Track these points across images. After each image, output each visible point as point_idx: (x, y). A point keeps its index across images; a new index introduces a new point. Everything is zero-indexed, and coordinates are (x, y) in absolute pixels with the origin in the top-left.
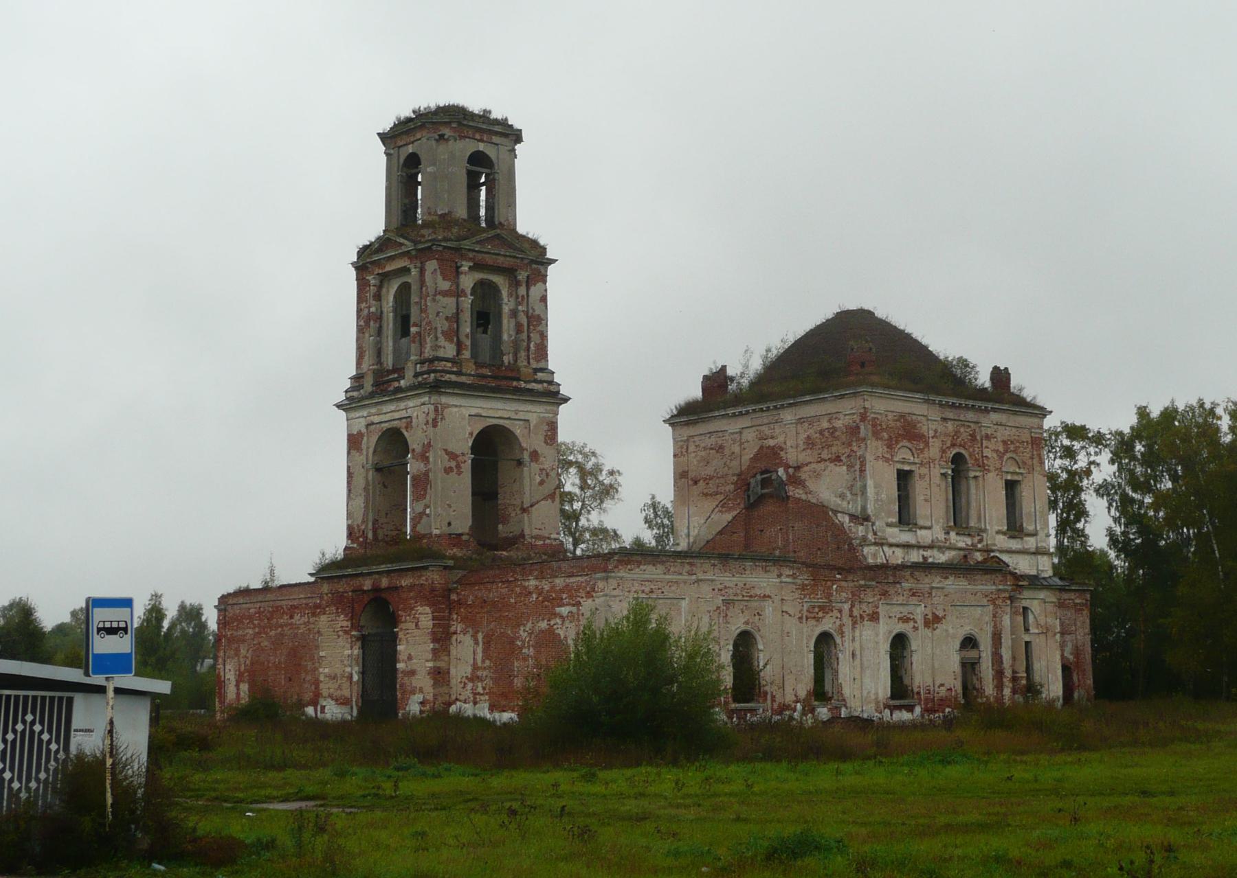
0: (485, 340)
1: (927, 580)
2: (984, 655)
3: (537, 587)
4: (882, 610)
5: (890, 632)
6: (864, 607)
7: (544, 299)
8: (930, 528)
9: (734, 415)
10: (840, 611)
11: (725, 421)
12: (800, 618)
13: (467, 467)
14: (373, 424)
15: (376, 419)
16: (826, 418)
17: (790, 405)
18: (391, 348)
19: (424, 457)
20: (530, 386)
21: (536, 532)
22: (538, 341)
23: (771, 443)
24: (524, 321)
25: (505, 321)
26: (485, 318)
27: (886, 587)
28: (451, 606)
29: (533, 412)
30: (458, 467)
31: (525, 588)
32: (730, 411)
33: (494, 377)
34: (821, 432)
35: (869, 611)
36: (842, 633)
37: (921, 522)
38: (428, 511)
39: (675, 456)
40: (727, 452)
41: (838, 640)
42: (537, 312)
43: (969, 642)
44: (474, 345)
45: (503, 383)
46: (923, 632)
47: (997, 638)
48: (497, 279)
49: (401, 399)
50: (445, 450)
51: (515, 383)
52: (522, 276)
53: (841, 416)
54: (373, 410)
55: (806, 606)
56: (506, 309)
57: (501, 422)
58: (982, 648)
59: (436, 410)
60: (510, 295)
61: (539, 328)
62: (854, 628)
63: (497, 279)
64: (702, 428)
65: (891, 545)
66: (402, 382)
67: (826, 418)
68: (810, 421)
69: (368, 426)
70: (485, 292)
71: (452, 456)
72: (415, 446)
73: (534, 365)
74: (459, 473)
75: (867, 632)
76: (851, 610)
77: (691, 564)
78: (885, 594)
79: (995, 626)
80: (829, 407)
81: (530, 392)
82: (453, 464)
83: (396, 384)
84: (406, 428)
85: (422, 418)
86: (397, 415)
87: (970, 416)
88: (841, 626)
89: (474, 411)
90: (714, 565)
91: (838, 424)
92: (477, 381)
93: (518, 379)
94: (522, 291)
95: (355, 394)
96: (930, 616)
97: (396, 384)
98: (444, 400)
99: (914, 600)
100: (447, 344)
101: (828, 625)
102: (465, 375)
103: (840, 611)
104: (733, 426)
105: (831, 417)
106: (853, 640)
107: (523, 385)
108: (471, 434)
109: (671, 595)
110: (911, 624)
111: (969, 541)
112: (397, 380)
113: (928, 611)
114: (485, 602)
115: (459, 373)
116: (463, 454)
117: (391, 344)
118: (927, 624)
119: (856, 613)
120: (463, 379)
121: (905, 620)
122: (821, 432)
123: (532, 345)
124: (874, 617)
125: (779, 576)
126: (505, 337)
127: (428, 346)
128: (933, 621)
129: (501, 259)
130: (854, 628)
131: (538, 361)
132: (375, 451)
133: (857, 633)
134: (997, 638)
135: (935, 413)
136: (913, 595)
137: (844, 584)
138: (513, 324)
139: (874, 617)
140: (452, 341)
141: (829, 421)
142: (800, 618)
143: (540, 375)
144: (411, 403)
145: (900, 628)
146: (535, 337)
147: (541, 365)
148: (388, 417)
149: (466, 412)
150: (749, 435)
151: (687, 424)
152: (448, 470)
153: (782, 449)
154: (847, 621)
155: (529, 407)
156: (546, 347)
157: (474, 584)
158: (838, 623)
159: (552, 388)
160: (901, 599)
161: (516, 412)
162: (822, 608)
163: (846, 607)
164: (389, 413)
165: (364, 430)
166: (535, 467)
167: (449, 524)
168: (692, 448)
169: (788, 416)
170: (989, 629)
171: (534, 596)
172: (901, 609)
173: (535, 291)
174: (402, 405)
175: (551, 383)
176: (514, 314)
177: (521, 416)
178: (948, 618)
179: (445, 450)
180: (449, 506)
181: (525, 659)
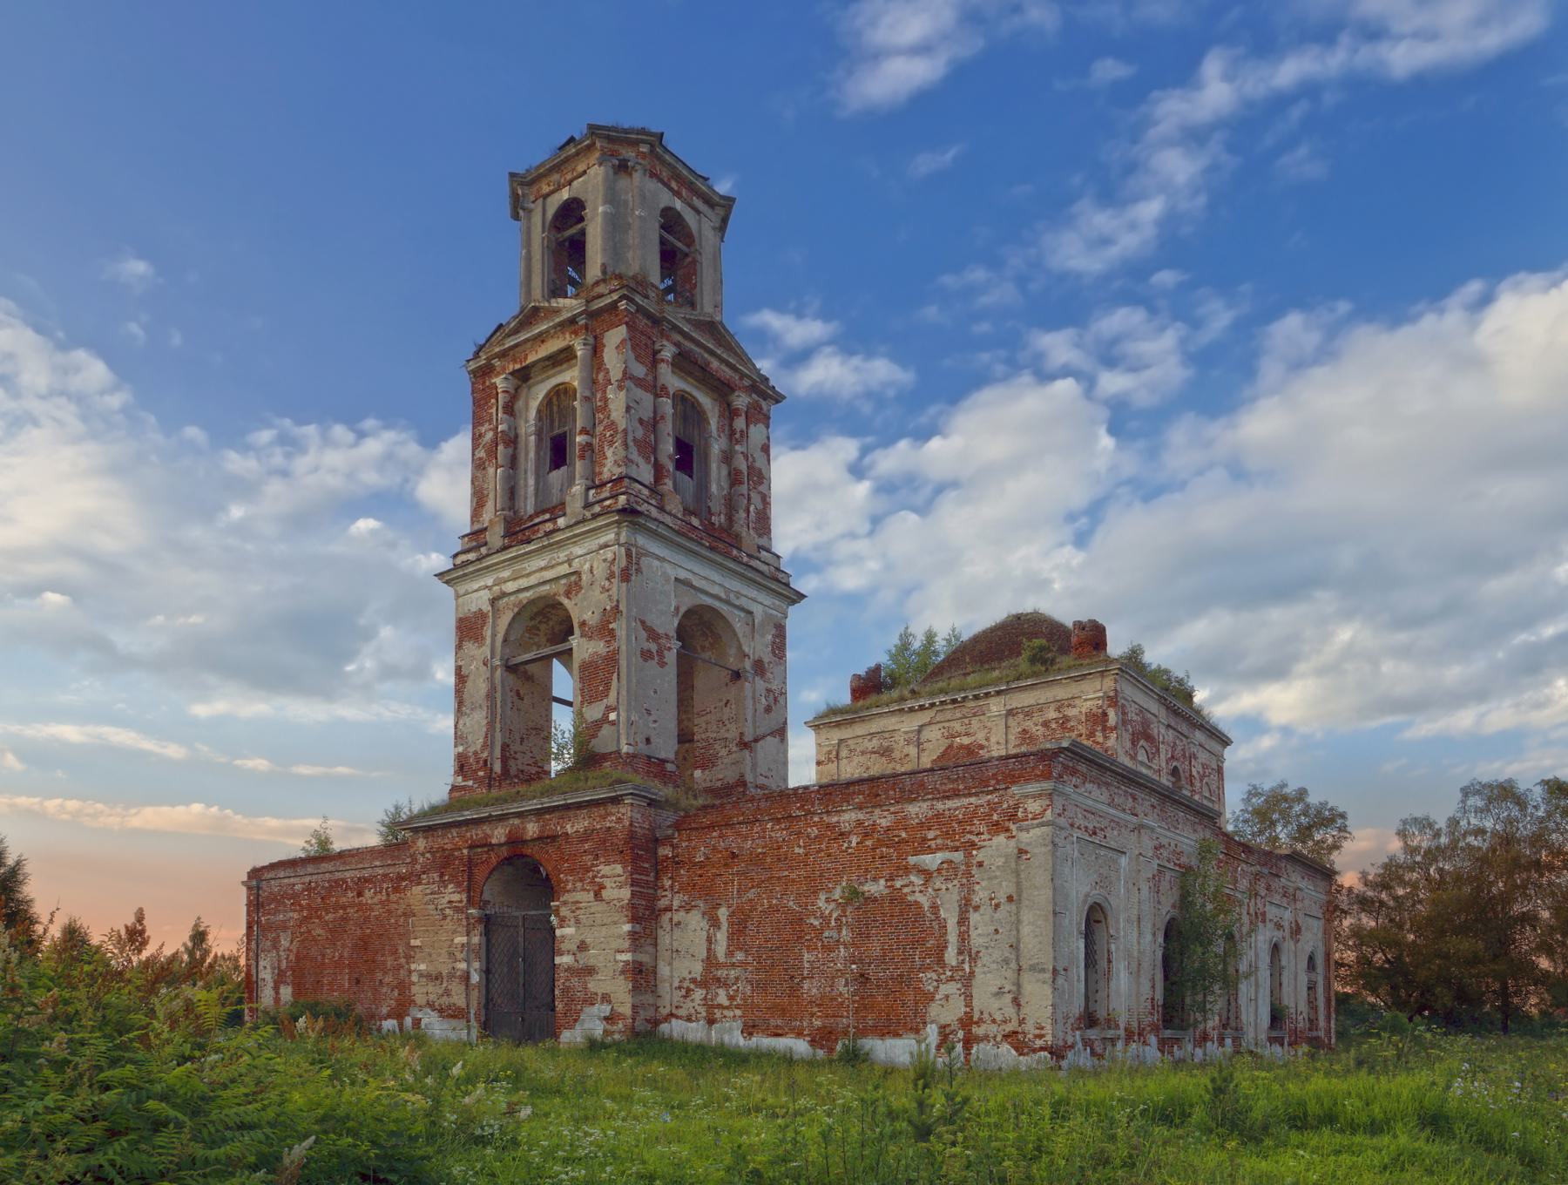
3: (860, 823)
9: (911, 710)
11: (894, 720)
13: (671, 657)
14: (504, 595)
15: (510, 587)
16: (1053, 706)
17: (999, 693)
18: (531, 489)
19: (604, 631)
21: (761, 781)
23: (966, 741)
25: (714, 466)
28: (659, 867)
30: (660, 653)
31: (829, 826)
32: (909, 704)
34: (1046, 724)
38: (612, 716)
39: (819, 763)
40: (896, 755)
48: (705, 400)
49: (560, 544)
50: (643, 623)
51: (735, 552)
52: (741, 400)
53: (1077, 702)
54: (506, 574)
56: (717, 447)
59: (629, 555)
60: (721, 429)
63: (705, 400)
64: (860, 730)
66: (561, 522)
67: (1053, 706)
68: (1028, 713)
69: (493, 601)
71: (653, 635)
72: (587, 616)
74: (662, 664)
80: (1060, 693)
82: (654, 647)
83: (549, 526)
84: (568, 594)
85: (600, 570)
86: (549, 575)
87: (1184, 728)
89: (683, 575)
91: (1071, 712)
94: (740, 423)
95: (471, 556)
97: (549, 526)
98: (641, 540)
100: (640, 461)
102: (670, 514)
104: (910, 724)
105: (1060, 705)
112: (553, 519)
114: (734, 855)
115: (661, 509)
117: (531, 482)
120: (668, 520)
122: (1046, 724)
126: (714, 488)
127: (609, 462)
129: (715, 364)
132: (505, 641)
135: (1162, 713)
138: (724, 472)
140: (647, 460)
141: (1058, 710)
144: (578, 550)
146: (756, 498)
148: (533, 580)
149: (672, 572)
150: (934, 735)
151: (838, 725)
152: (646, 655)
153: (982, 747)
157: (711, 827)
164: (533, 573)
165: (486, 608)
166: (760, 684)
167: (648, 740)
168: (844, 753)
169: (996, 706)
171: (854, 840)
174: (562, 555)
176: (727, 458)
179: (643, 623)
180: (649, 712)
181: (828, 949)
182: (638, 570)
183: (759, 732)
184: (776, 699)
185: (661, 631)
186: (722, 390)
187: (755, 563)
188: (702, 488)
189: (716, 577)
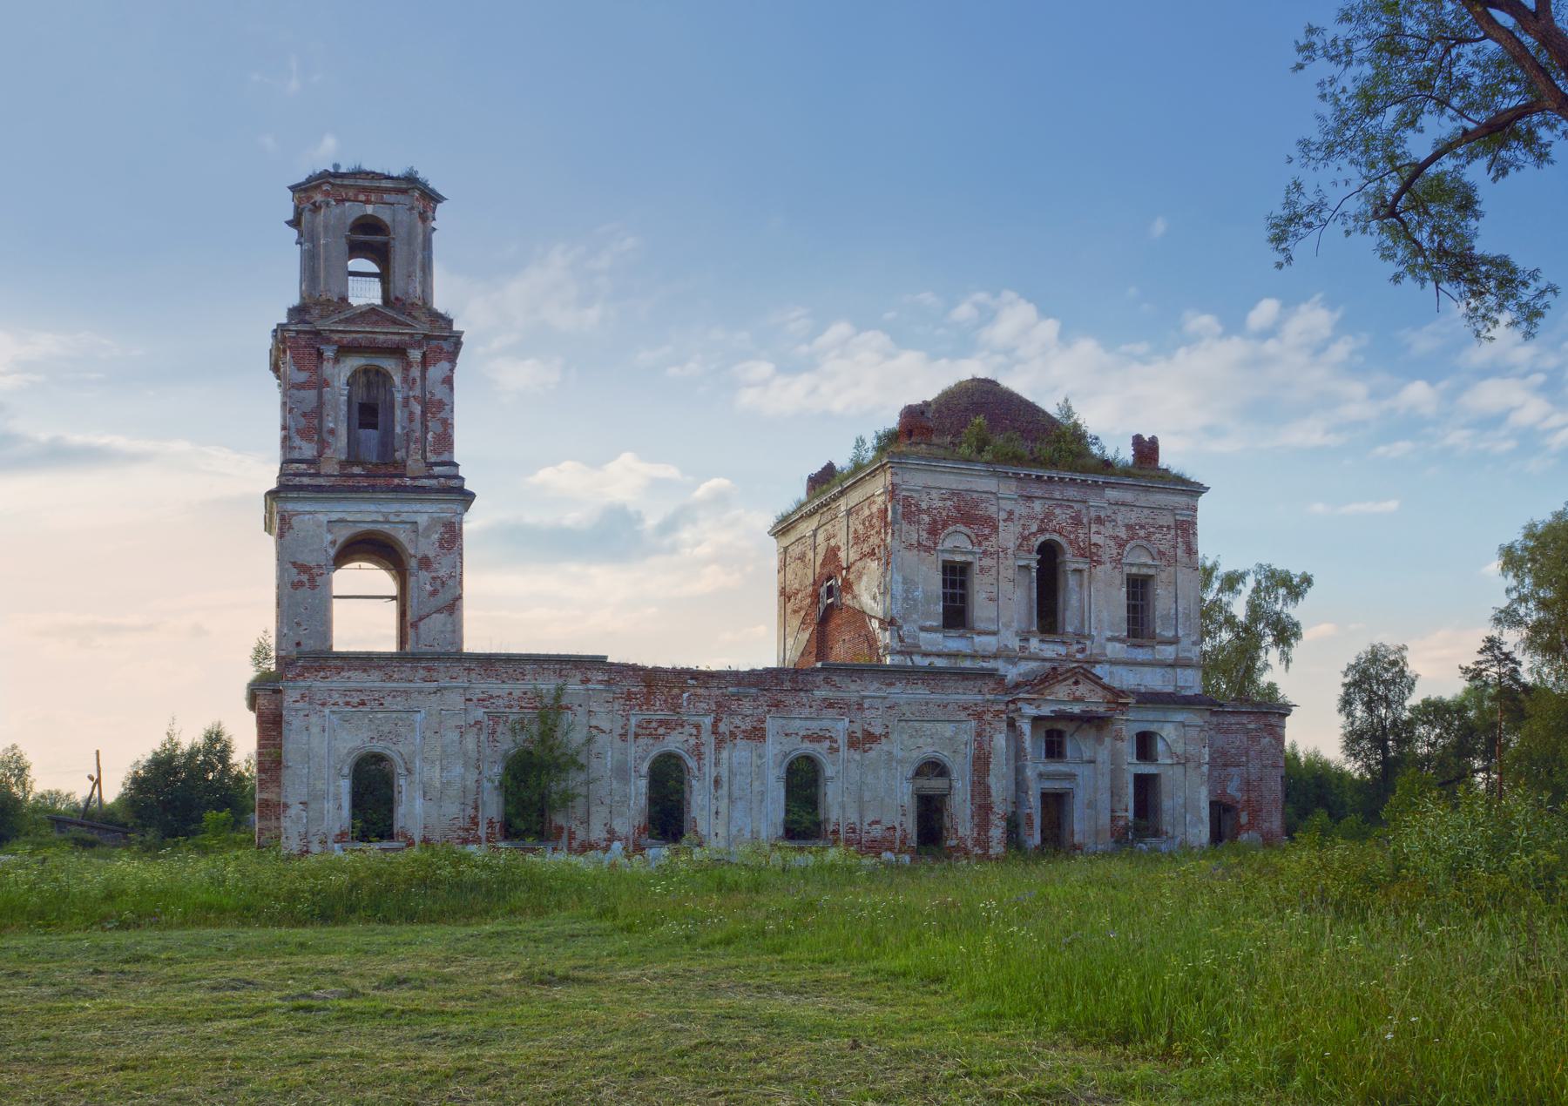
0: (370, 436)
1: (853, 687)
2: (958, 785)
4: (771, 725)
5: (786, 755)
6: (737, 721)
7: (448, 381)
8: (994, 633)
10: (698, 727)
12: (623, 736)
20: (419, 483)
22: (440, 430)
24: (417, 409)
25: (398, 413)
26: (369, 412)
27: (780, 697)
29: (424, 513)
30: (312, 580)
33: (367, 476)
35: (747, 725)
36: (700, 757)
37: (980, 625)
41: (692, 763)
42: (438, 397)
43: (934, 768)
44: (352, 442)
45: (380, 482)
46: (844, 752)
47: (981, 763)
50: (294, 564)
51: (396, 481)
52: (415, 355)
55: (633, 721)
56: (398, 397)
57: (379, 527)
58: (954, 775)
60: (405, 380)
61: (442, 415)
62: (718, 748)
63: (389, 365)
65: (926, 655)
70: (373, 379)
71: (303, 568)
73: (432, 458)
75: (740, 753)
76: (715, 725)
77: (429, 669)
78: (777, 705)
79: (980, 746)
81: (423, 489)
82: (305, 578)
88: (697, 745)
89: (334, 517)
90: (469, 669)
92: (339, 482)
93: (402, 476)
94: (416, 372)
96: (859, 734)
99: (832, 712)
101: (674, 742)
103: (698, 727)
106: (717, 764)
107: (408, 482)
108: (333, 543)
109: (395, 707)
110: (827, 744)
111: (1062, 650)
113: (857, 727)
116: (319, 566)
118: (853, 743)
119: (722, 728)
121: (815, 738)
123: (430, 436)
124: (757, 734)
125: (585, 681)
126: (398, 430)
128: (863, 741)
129: (381, 337)
130: (718, 748)
131: (440, 454)
133: (725, 754)
134: (981, 763)
136: (831, 706)
137: (700, 691)
139: (757, 734)
142: (623, 736)
143: (437, 470)
145: (807, 748)
147: (445, 457)
149: (323, 518)
152: (297, 585)
154: (708, 738)
155: (417, 507)
156: (451, 436)
158: (693, 741)
159: (453, 483)
160: (806, 712)
161: (397, 514)
162: (661, 723)
163: (707, 721)
167: (298, 644)
170: (970, 751)
172: (808, 724)
173: (436, 372)
175: (457, 477)
177: (404, 517)
178: (894, 736)
179: (294, 564)
182: (291, 527)
183: (422, 613)
184: (443, 583)
185: (313, 564)
186: (398, 351)
187: (426, 482)
188: (389, 431)
189: (372, 508)
